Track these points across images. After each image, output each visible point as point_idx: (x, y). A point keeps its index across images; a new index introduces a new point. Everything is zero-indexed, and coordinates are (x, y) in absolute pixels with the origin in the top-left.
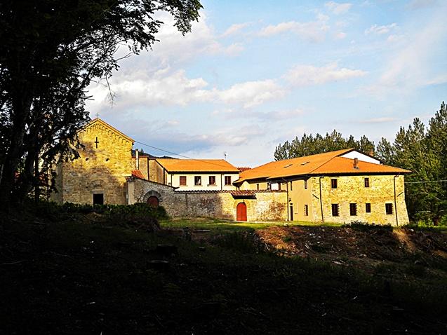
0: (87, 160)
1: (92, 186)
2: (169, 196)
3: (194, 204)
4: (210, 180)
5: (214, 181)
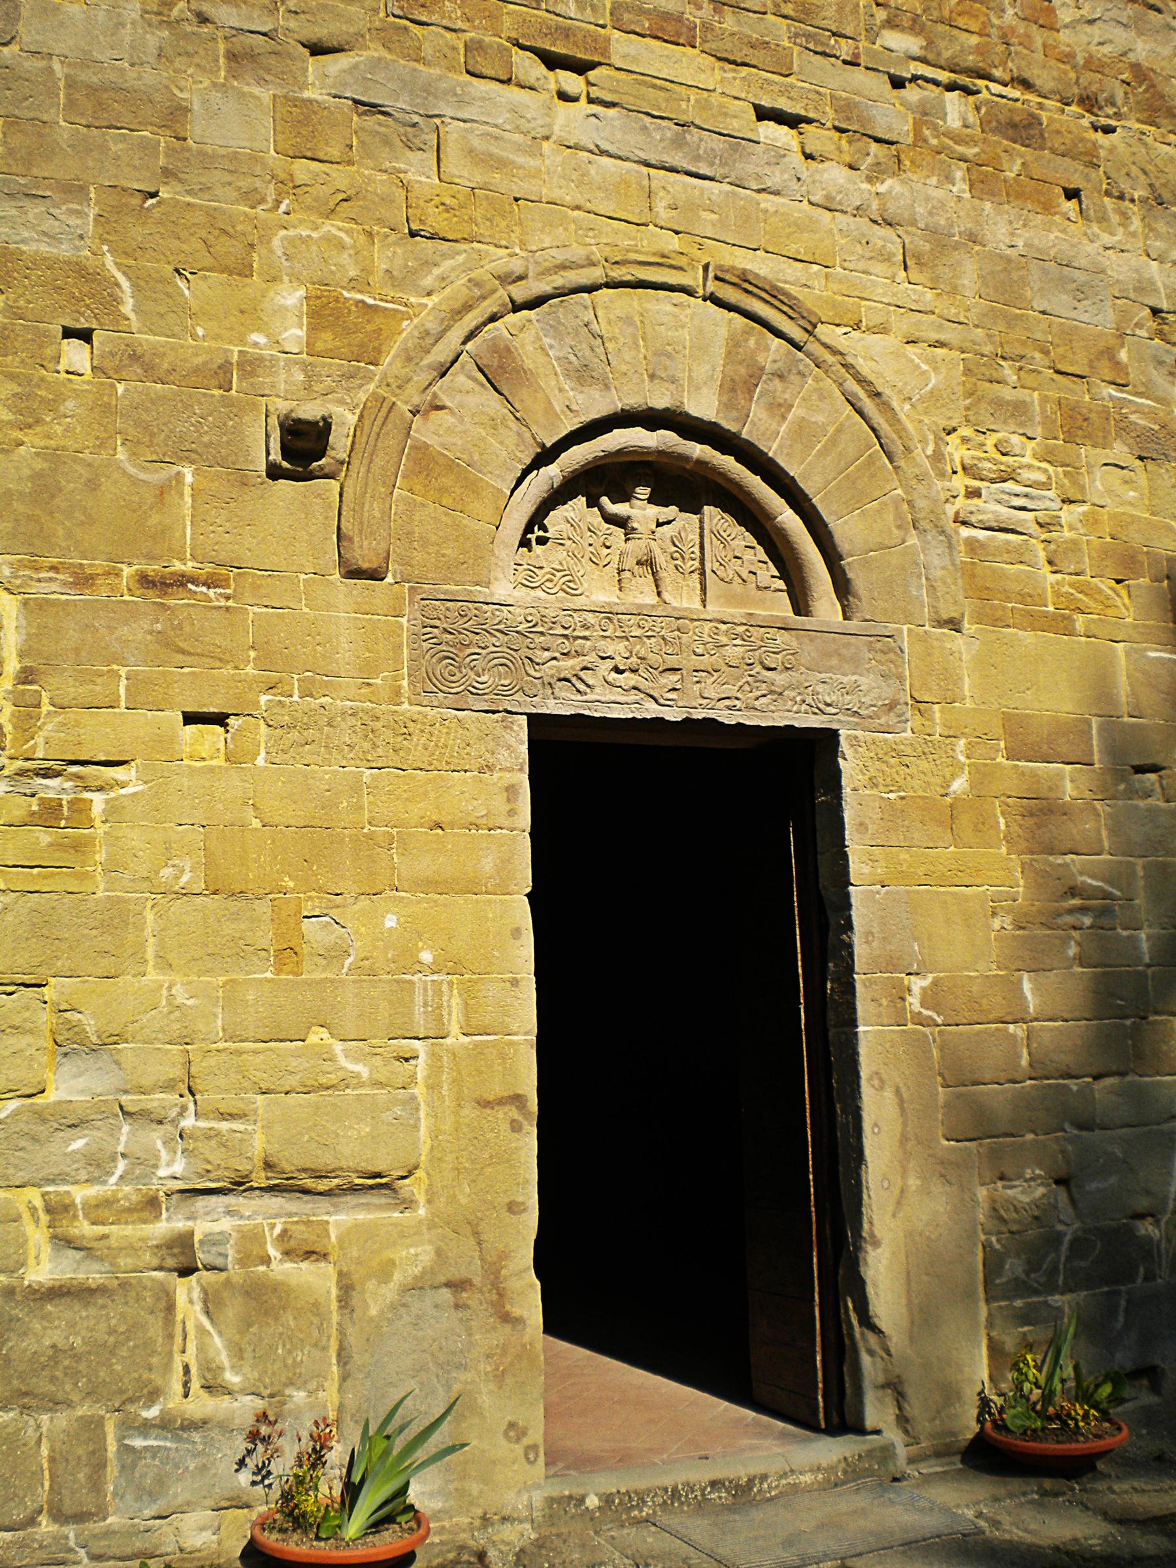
1: (479, 432)
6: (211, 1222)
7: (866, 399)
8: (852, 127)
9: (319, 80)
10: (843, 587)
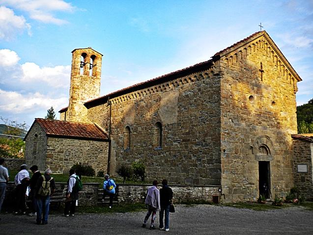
0: (251, 97)
1: (257, 146)
6: (248, 185)
7: (272, 143)
8: (272, 125)
10: (270, 153)
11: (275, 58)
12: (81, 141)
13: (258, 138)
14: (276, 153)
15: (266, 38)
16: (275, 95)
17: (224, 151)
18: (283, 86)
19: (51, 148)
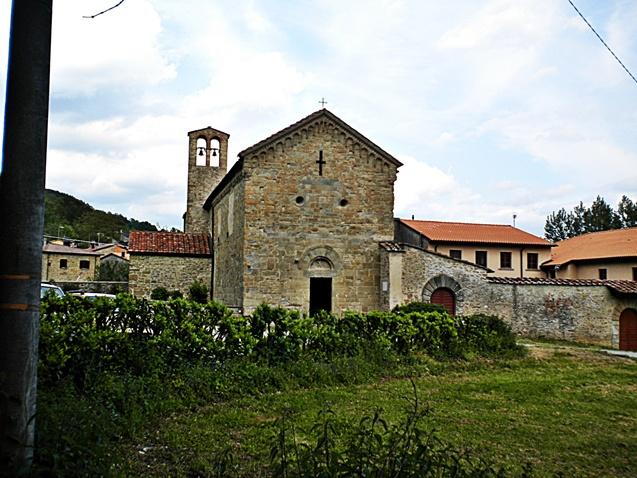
1: (307, 259)
2: (476, 290)
3: (530, 309)
4: (502, 260)
5: (509, 260)
7: (337, 254)
8: (338, 231)
9: (298, 236)
11: (350, 142)
12: (173, 259)
13: (310, 249)
14: (345, 267)
15: (328, 117)
16: (347, 190)
17: (249, 267)
18: (366, 176)
19: (134, 268)
